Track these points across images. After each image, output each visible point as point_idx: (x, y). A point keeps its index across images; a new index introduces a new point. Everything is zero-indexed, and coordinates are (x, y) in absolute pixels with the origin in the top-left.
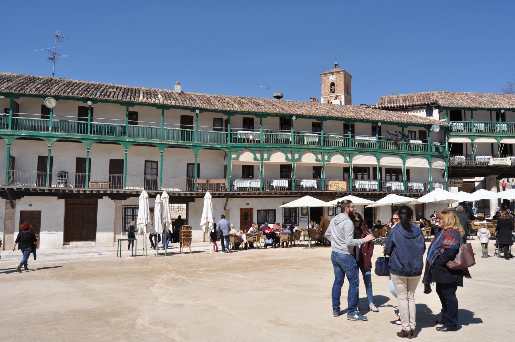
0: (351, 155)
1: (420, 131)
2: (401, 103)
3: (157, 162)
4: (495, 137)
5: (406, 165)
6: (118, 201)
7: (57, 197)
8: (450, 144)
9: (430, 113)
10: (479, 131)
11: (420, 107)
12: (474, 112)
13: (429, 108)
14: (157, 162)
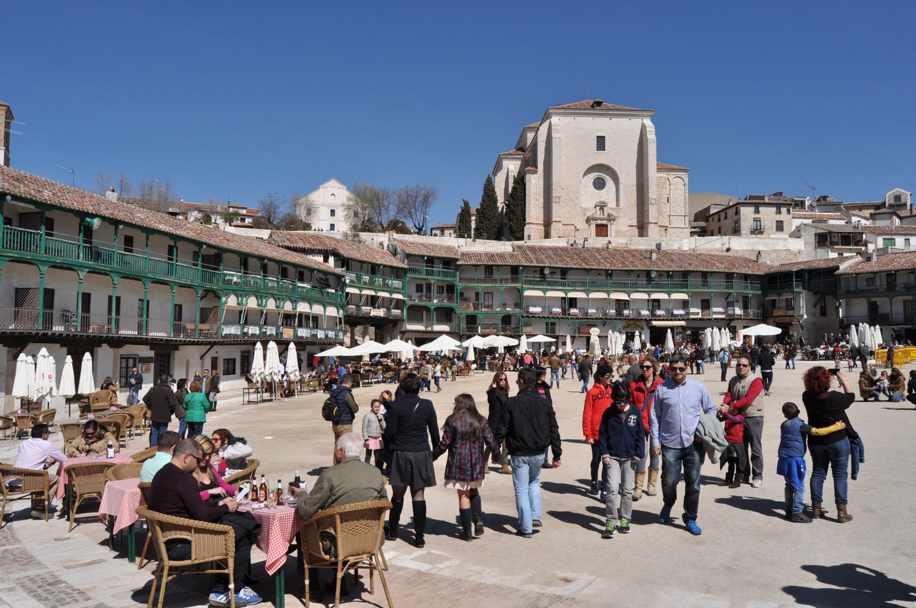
0: (294, 302)
2: (301, 245)
4: (375, 290)
5: (327, 314)
6: (116, 350)
7: (59, 345)
8: (347, 294)
9: (326, 260)
10: (365, 283)
11: (319, 252)
13: (326, 255)
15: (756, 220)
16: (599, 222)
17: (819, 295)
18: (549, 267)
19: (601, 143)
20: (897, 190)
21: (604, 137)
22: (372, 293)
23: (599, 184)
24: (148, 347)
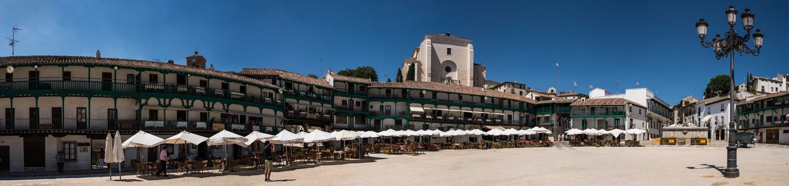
1: (269, 93)
3: (86, 108)
9: (274, 83)
12: (300, 85)
14: (86, 108)
18: (426, 90)
24: (86, 136)
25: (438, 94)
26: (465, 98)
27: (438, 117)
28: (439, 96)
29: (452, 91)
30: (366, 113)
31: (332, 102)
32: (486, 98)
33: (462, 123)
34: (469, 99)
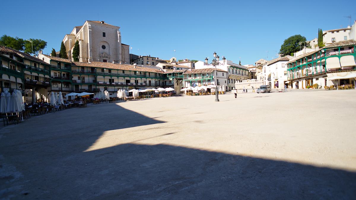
15: (147, 61)
16: (104, 59)
17: (177, 80)
18: (106, 68)
19: (104, 35)
20: (174, 58)
21: (105, 33)
22: (37, 75)
23: (104, 47)
25: (112, 71)
26: (126, 73)
27: (113, 83)
28: (113, 72)
29: (119, 69)
30: (71, 81)
31: (49, 74)
32: (137, 72)
33: (125, 86)
34: (128, 73)
